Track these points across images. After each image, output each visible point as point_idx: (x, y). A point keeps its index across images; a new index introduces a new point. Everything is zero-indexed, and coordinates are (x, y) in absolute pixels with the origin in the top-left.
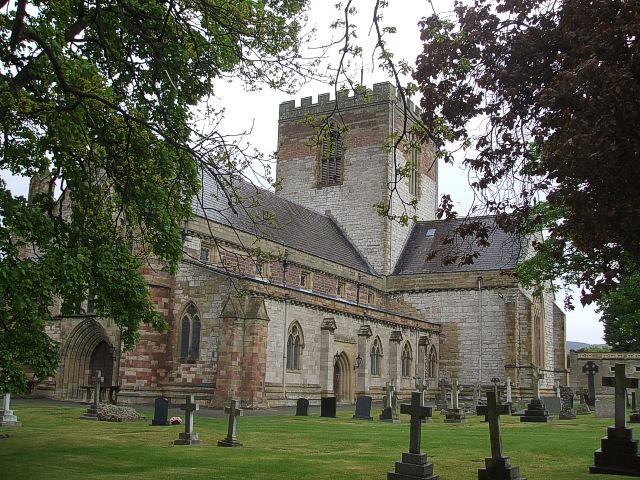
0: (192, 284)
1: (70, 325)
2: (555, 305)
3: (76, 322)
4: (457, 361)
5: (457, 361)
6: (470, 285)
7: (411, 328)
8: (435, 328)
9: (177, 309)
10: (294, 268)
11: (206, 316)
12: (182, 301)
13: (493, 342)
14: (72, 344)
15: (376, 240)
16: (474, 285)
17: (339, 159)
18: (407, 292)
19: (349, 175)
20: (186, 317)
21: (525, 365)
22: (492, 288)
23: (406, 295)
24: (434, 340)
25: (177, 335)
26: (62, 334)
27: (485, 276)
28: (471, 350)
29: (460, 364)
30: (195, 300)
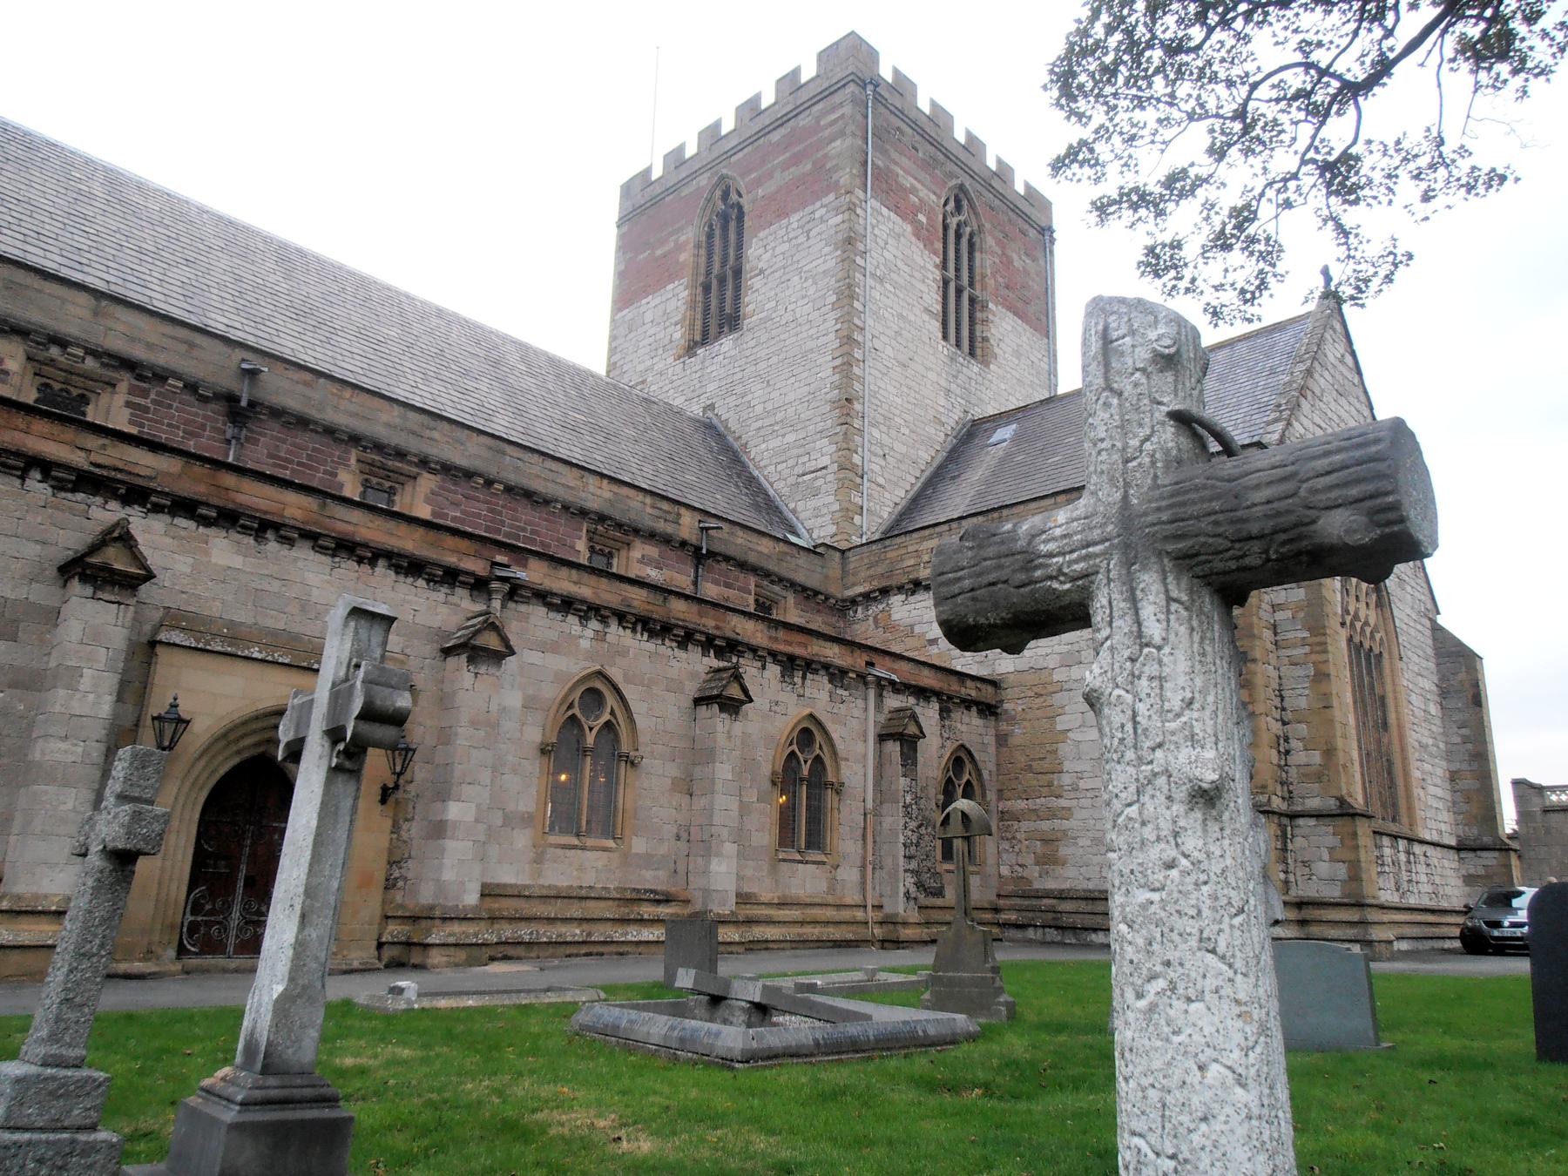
2: (1437, 629)
7: (837, 675)
8: (970, 691)
10: (304, 438)
15: (824, 453)
17: (738, 273)
18: (900, 589)
19: (758, 297)
21: (1313, 803)
23: (896, 600)
24: (969, 727)
29: (1067, 813)
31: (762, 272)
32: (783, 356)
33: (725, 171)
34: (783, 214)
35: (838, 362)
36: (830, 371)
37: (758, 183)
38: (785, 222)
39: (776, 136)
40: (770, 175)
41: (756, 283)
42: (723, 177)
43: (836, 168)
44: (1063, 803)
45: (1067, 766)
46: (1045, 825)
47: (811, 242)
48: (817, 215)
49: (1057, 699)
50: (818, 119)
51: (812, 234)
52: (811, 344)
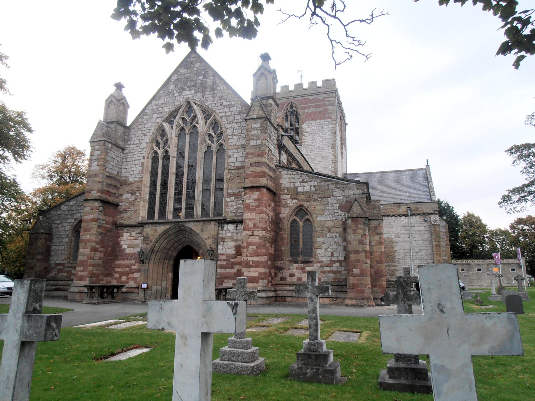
0: (300, 189)
1: (156, 230)
3: (161, 229)
4: (394, 264)
5: (394, 264)
6: (402, 213)
9: (285, 213)
11: (320, 218)
12: (290, 205)
13: (420, 251)
14: (156, 248)
16: (405, 213)
17: (297, 129)
20: (294, 220)
22: (419, 214)
25: (286, 234)
26: (146, 239)
27: (413, 207)
28: (404, 257)
29: (397, 266)
30: (305, 204)
31: (307, 132)
32: (316, 156)
33: (292, 101)
34: (314, 119)
35: (334, 161)
36: (331, 163)
37: (305, 108)
38: (315, 121)
39: (310, 98)
40: (309, 108)
41: (306, 135)
42: (292, 102)
43: (331, 113)
44: (396, 264)
45: (396, 257)
46: (392, 268)
47: (323, 130)
48: (325, 123)
49: (394, 244)
50: (324, 99)
51: (324, 127)
52: (324, 155)
